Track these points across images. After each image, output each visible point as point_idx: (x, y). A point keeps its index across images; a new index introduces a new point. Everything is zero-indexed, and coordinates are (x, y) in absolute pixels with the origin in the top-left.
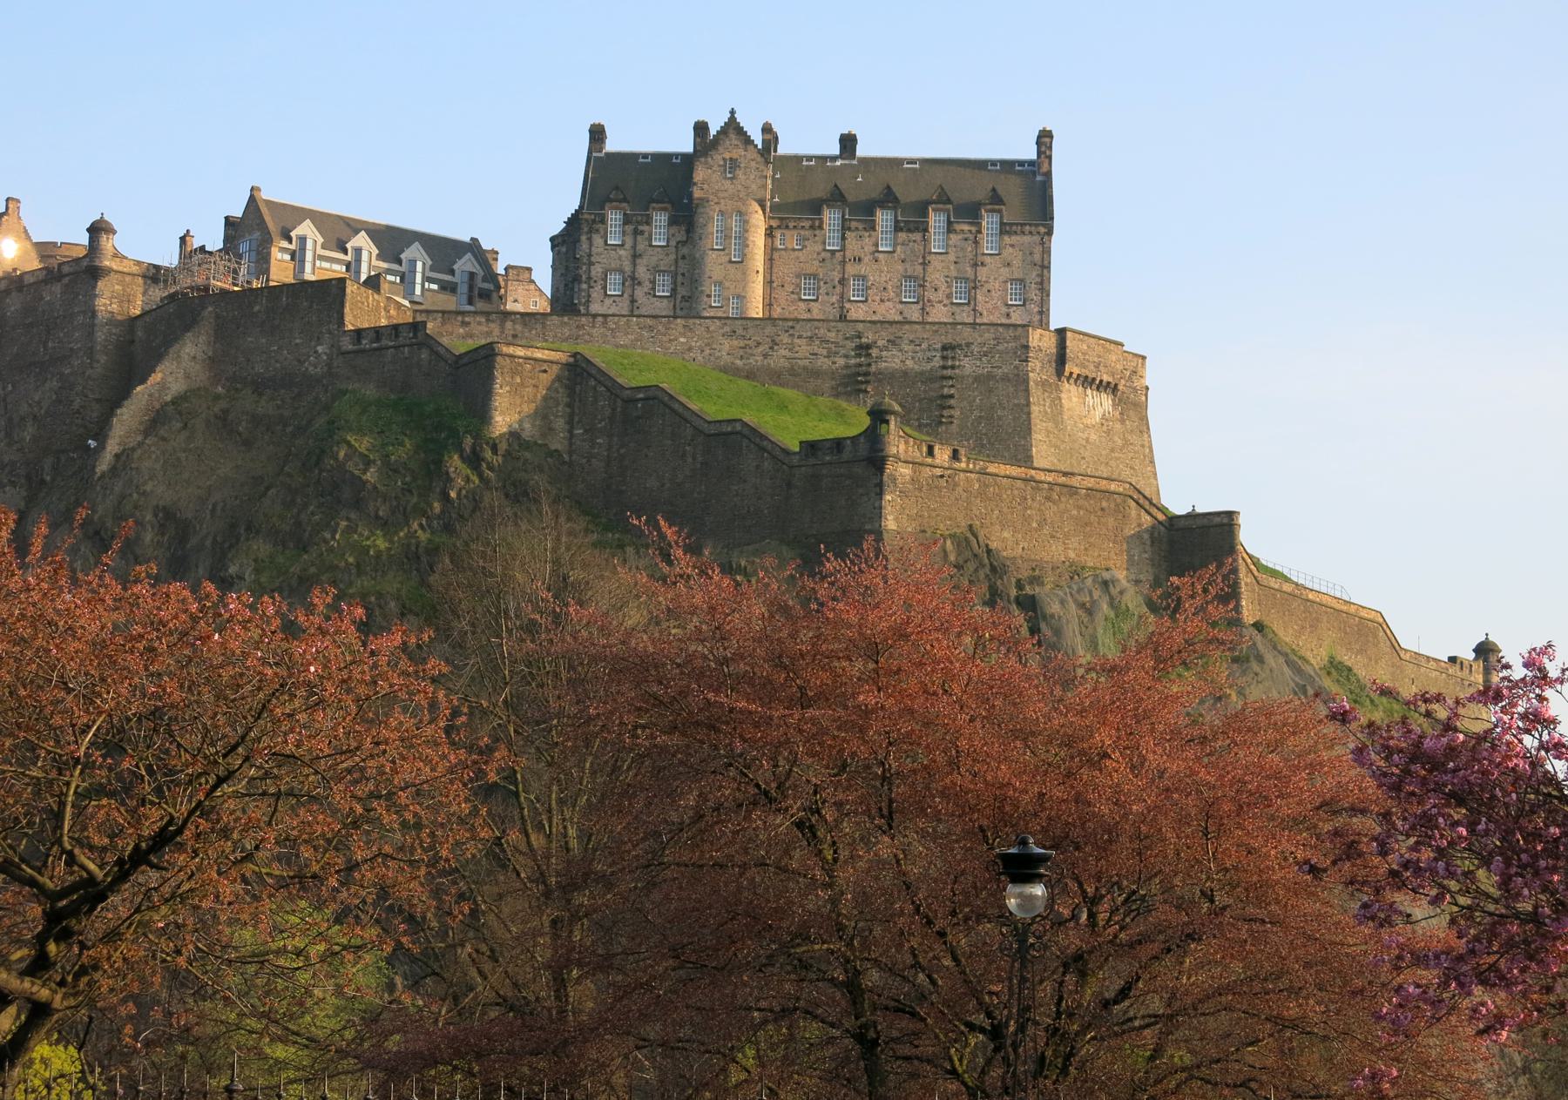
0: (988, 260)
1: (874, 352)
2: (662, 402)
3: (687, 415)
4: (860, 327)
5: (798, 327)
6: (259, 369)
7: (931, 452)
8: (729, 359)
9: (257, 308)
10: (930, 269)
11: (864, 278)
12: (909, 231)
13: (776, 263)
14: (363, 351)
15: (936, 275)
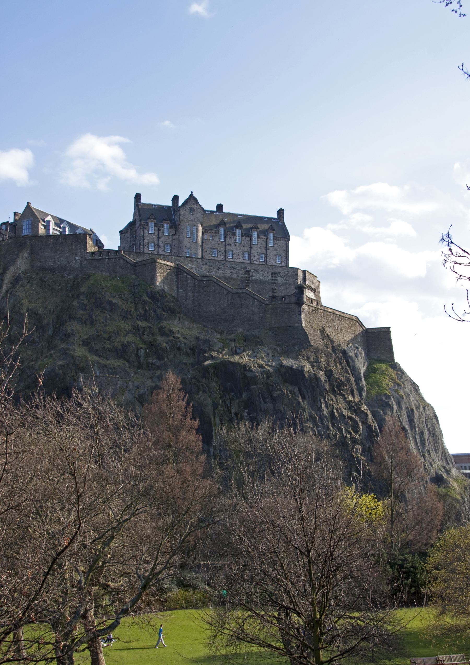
0: (270, 248)
1: (251, 273)
2: (214, 282)
3: (223, 286)
4: (246, 265)
5: (226, 263)
6: (51, 264)
7: (312, 303)
8: (205, 272)
9: (49, 242)
10: (252, 249)
11: (232, 250)
12: (246, 236)
13: (204, 244)
14: (96, 259)
15: (254, 252)
